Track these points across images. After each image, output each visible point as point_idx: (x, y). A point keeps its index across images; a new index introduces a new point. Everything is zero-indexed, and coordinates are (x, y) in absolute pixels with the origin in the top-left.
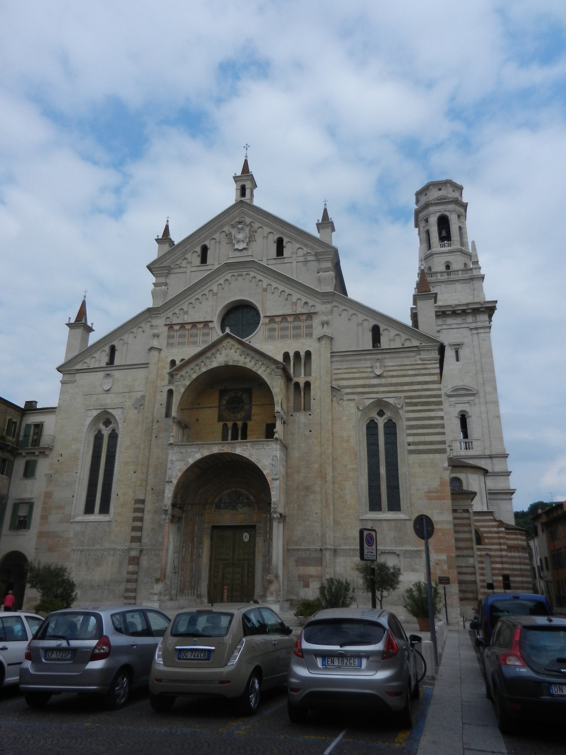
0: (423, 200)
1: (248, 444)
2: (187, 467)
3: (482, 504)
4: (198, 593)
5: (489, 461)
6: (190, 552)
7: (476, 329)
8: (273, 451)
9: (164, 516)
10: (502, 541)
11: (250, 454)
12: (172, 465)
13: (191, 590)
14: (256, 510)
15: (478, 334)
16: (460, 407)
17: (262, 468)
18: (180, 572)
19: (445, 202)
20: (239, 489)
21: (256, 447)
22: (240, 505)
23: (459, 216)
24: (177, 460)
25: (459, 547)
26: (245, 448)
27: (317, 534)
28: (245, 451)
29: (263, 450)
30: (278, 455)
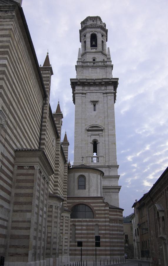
0: (84, 26)
3: (97, 193)
5: (107, 169)
7: (106, 93)
10: (106, 216)
15: (107, 96)
16: (93, 138)
19: (95, 27)
23: (102, 36)
25: (20, 202)
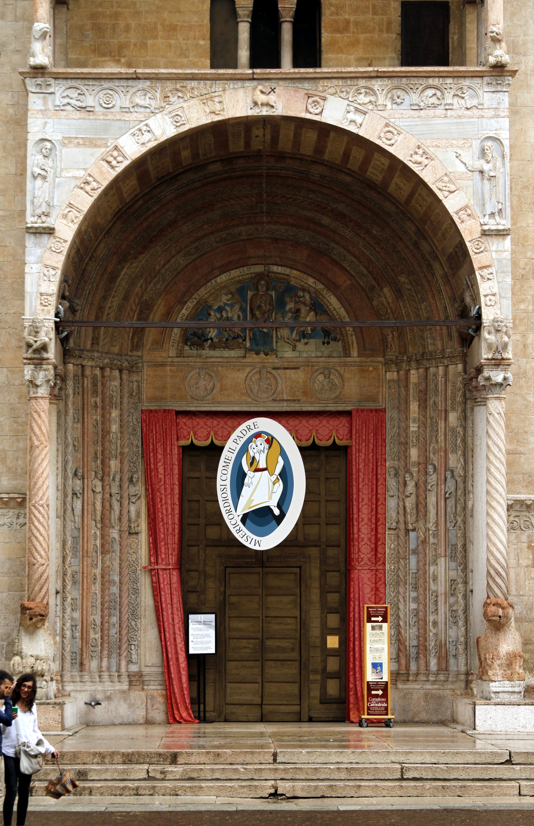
1: (376, 85)
2: (114, 174)
4: (134, 668)
6: (98, 518)
8: (483, 117)
9: (28, 371)
11: (387, 125)
12: (50, 162)
13: (109, 657)
17: (440, 185)
18: (69, 587)
20: (275, 268)
21: (414, 98)
22: (285, 332)
24: (67, 141)
26: (363, 99)
28: (365, 113)
29: (440, 111)
30: (505, 136)
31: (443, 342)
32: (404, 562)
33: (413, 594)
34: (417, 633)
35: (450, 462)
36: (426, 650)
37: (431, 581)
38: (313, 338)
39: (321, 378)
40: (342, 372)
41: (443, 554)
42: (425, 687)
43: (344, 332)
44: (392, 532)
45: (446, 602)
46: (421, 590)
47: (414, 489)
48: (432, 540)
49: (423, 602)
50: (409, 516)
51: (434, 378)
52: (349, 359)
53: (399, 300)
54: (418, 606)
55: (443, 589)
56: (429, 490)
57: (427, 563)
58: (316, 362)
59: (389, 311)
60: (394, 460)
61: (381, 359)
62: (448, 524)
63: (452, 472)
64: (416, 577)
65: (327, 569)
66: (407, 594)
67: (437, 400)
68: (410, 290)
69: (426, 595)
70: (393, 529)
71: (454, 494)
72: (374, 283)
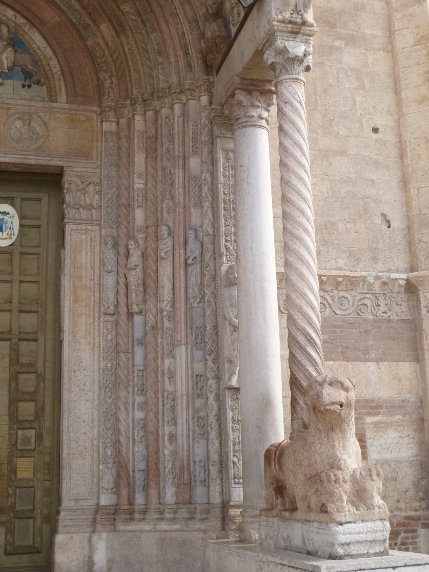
14: (63, 97)
27: (384, 216)
31: (179, 77)
32: (126, 356)
33: (139, 399)
34: (144, 452)
35: (193, 219)
36: (158, 476)
37: (166, 379)
38: (11, 79)
39: (19, 124)
40: (47, 119)
41: (183, 342)
42: (158, 527)
43: (50, 76)
44: (108, 318)
45: (188, 407)
46: (151, 393)
47: (140, 259)
48: (167, 324)
49: (154, 408)
50: (134, 295)
51: (167, 120)
52: (55, 105)
53: (121, 35)
54: (147, 414)
55: (184, 388)
56: (163, 259)
57: (159, 355)
58: (13, 104)
59: (107, 53)
60: (112, 228)
61: (96, 108)
62: (191, 300)
63: (196, 230)
64: (142, 376)
65: (20, 371)
66: (130, 400)
67: (171, 147)
68: (136, 21)
69: (158, 399)
70: (110, 314)
71: (199, 259)
72: (88, 20)
